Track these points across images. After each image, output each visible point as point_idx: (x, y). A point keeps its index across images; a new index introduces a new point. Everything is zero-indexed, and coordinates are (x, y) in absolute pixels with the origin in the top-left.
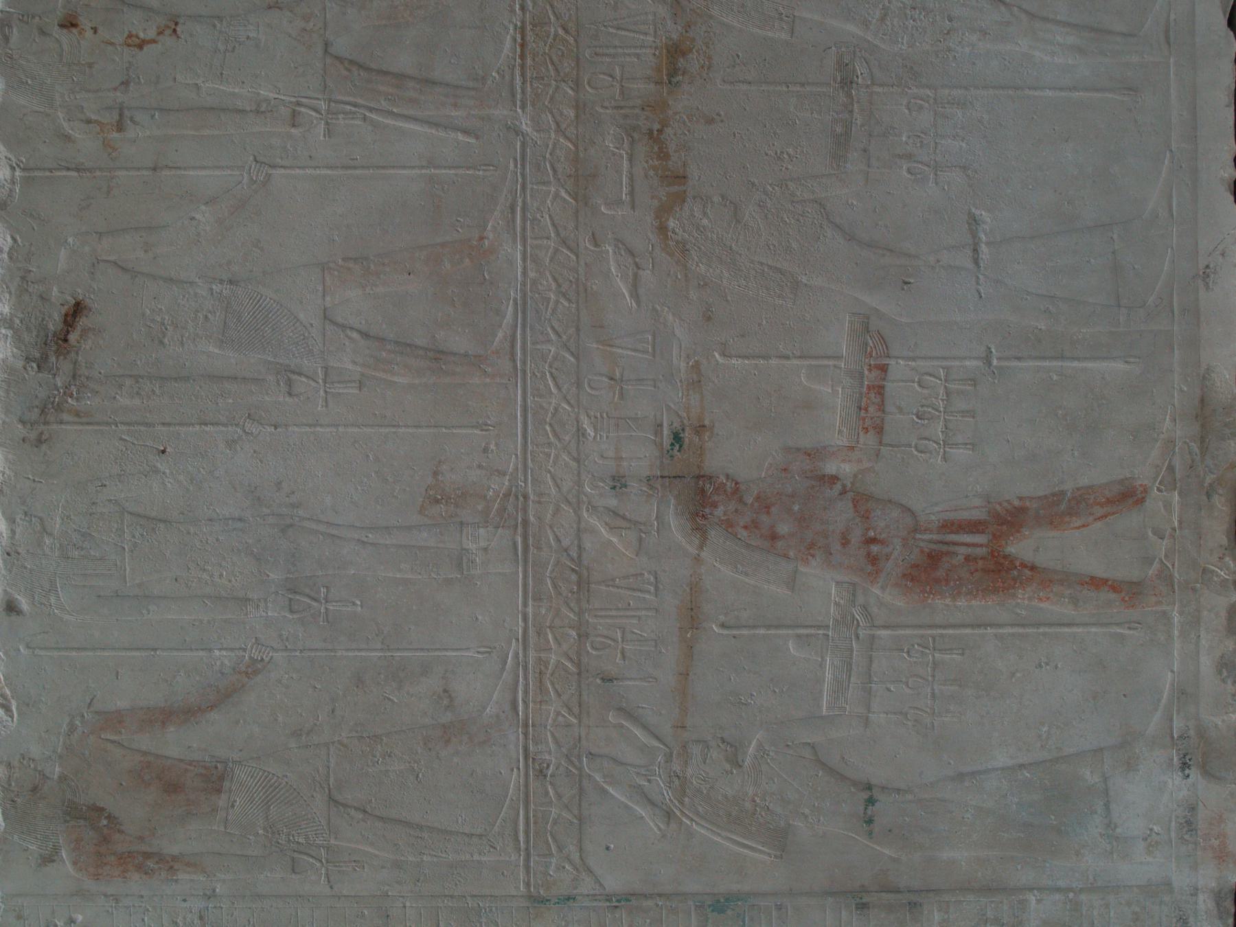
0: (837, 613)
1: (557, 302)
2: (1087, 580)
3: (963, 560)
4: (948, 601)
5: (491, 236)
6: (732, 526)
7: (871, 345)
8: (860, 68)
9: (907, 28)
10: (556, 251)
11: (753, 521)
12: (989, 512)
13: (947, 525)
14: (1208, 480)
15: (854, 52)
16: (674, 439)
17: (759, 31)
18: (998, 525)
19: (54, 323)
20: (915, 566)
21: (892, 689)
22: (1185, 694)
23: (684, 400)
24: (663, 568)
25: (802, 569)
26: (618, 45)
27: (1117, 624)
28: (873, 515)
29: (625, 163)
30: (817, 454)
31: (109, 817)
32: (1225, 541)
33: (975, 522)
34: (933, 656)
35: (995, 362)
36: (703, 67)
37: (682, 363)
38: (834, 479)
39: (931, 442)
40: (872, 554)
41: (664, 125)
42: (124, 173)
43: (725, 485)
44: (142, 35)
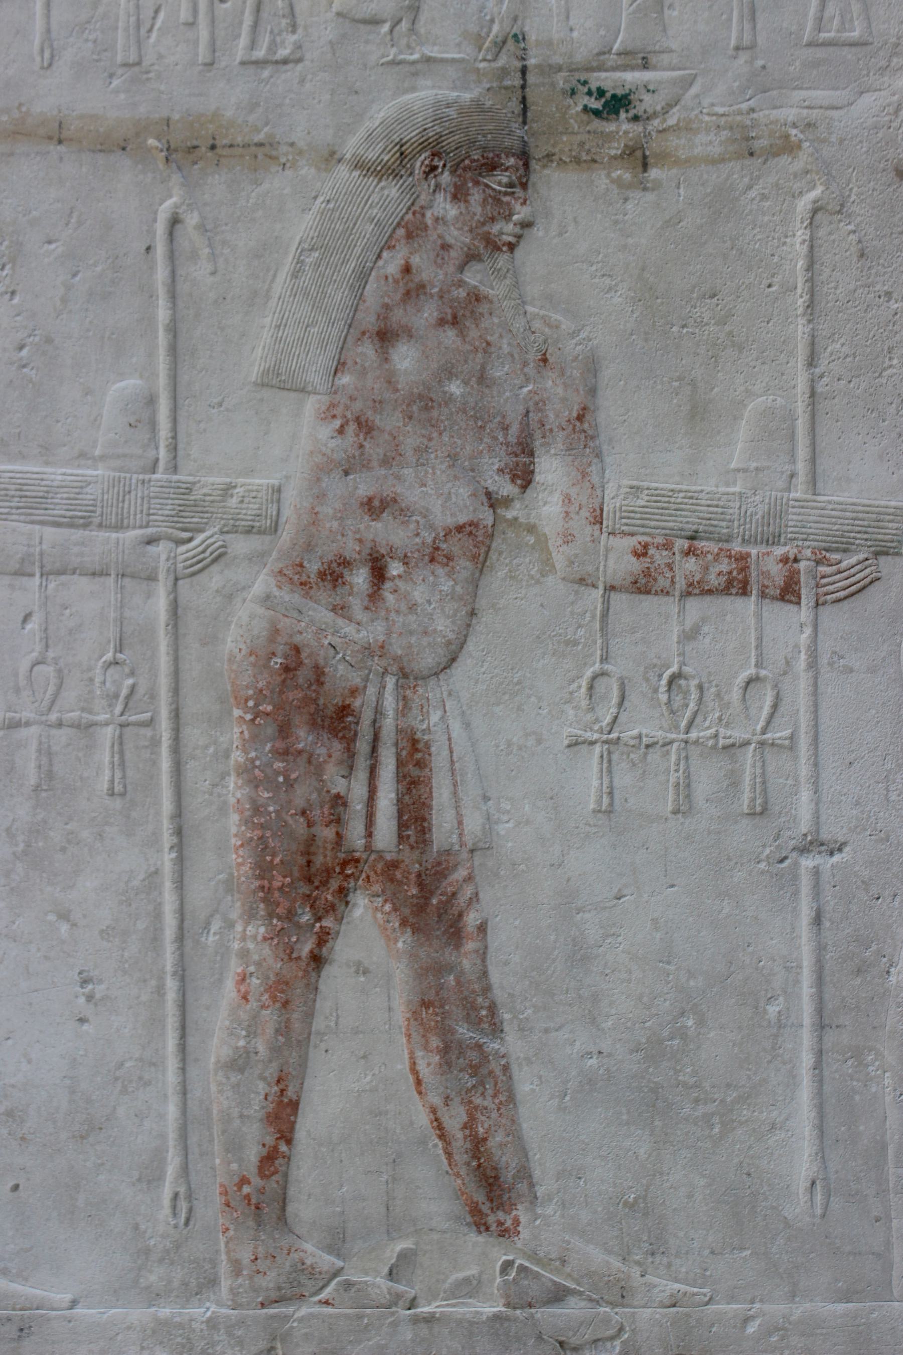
0: (205, 490)
2: (291, 1093)
3: (334, 791)
4: (237, 757)
6: (409, 236)
7: (844, 565)
11: (422, 287)
12: (448, 852)
13: (417, 750)
16: (614, 96)
18: (419, 875)
20: (319, 674)
21: (29, 627)
23: (707, 118)
24: (310, 77)
25: (311, 405)
27: (185, 1169)
28: (440, 571)
30: (582, 436)
33: (424, 819)
34: (107, 724)
35: (807, 862)
37: (794, 111)
39: (614, 710)
40: (346, 573)
43: (508, 217)
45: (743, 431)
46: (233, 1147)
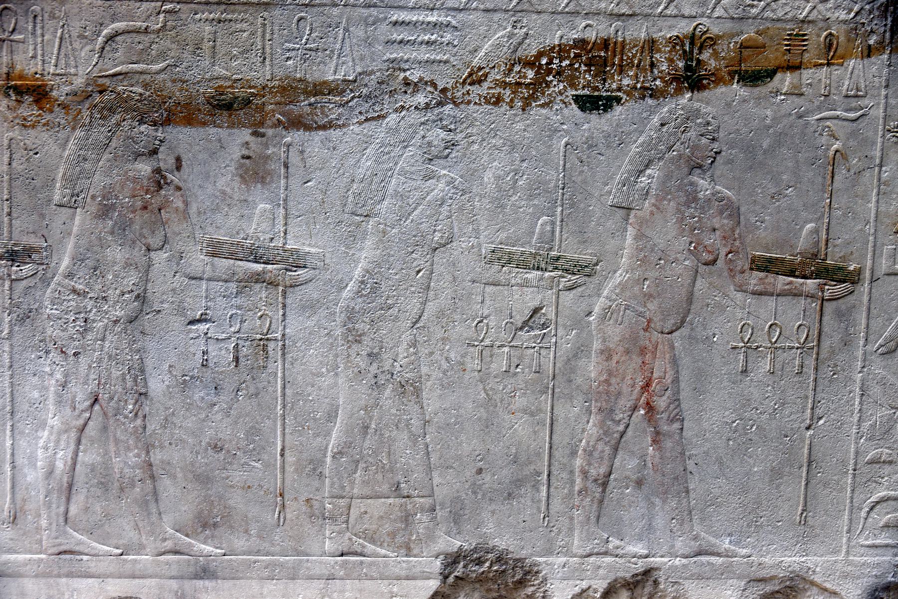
8: (27, 269)
9: (66, 314)
15: (43, 264)
17: (60, 175)
26: (45, 38)
36: (25, 119)
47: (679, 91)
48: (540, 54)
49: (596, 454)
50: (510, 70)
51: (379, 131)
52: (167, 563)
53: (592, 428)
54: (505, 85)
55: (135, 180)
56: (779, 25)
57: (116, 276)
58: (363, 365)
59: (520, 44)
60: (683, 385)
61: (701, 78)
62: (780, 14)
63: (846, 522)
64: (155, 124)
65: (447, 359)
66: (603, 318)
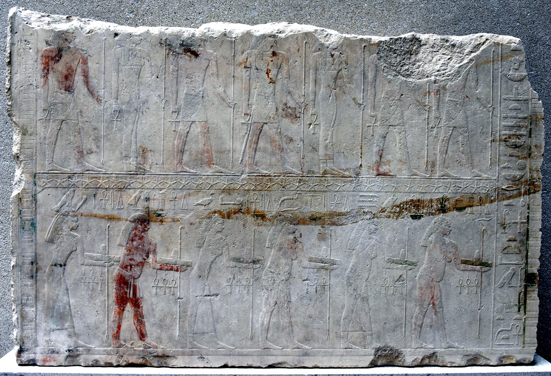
1: (196, 184)
4: (115, 287)
5: (214, 167)
8: (258, 266)
10: (210, 184)
14: (147, 358)
19: (193, 48)
20: (124, 278)
22: (89, 351)
25: (124, 248)
27: (108, 333)
29: (233, 203)
31: (58, 61)
32: (130, 362)
35: (179, 300)
38: (148, 257)
41: (243, 213)
42: (233, 68)
44: (270, 73)
45: (172, 252)
46: (113, 330)
47: (439, 213)
48: (401, 204)
49: (418, 318)
50: (393, 208)
51: (356, 226)
52: (295, 351)
53: (417, 310)
54: (391, 212)
55: (289, 240)
56: (466, 194)
57: (283, 267)
58: (352, 292)
59: (395, 201)
60: (443, 297)
61: (445, 210)
62: (467, 191)
63: (491, 337)
64: (294, 224)
65: (376, 290)
66: (420, 278)
